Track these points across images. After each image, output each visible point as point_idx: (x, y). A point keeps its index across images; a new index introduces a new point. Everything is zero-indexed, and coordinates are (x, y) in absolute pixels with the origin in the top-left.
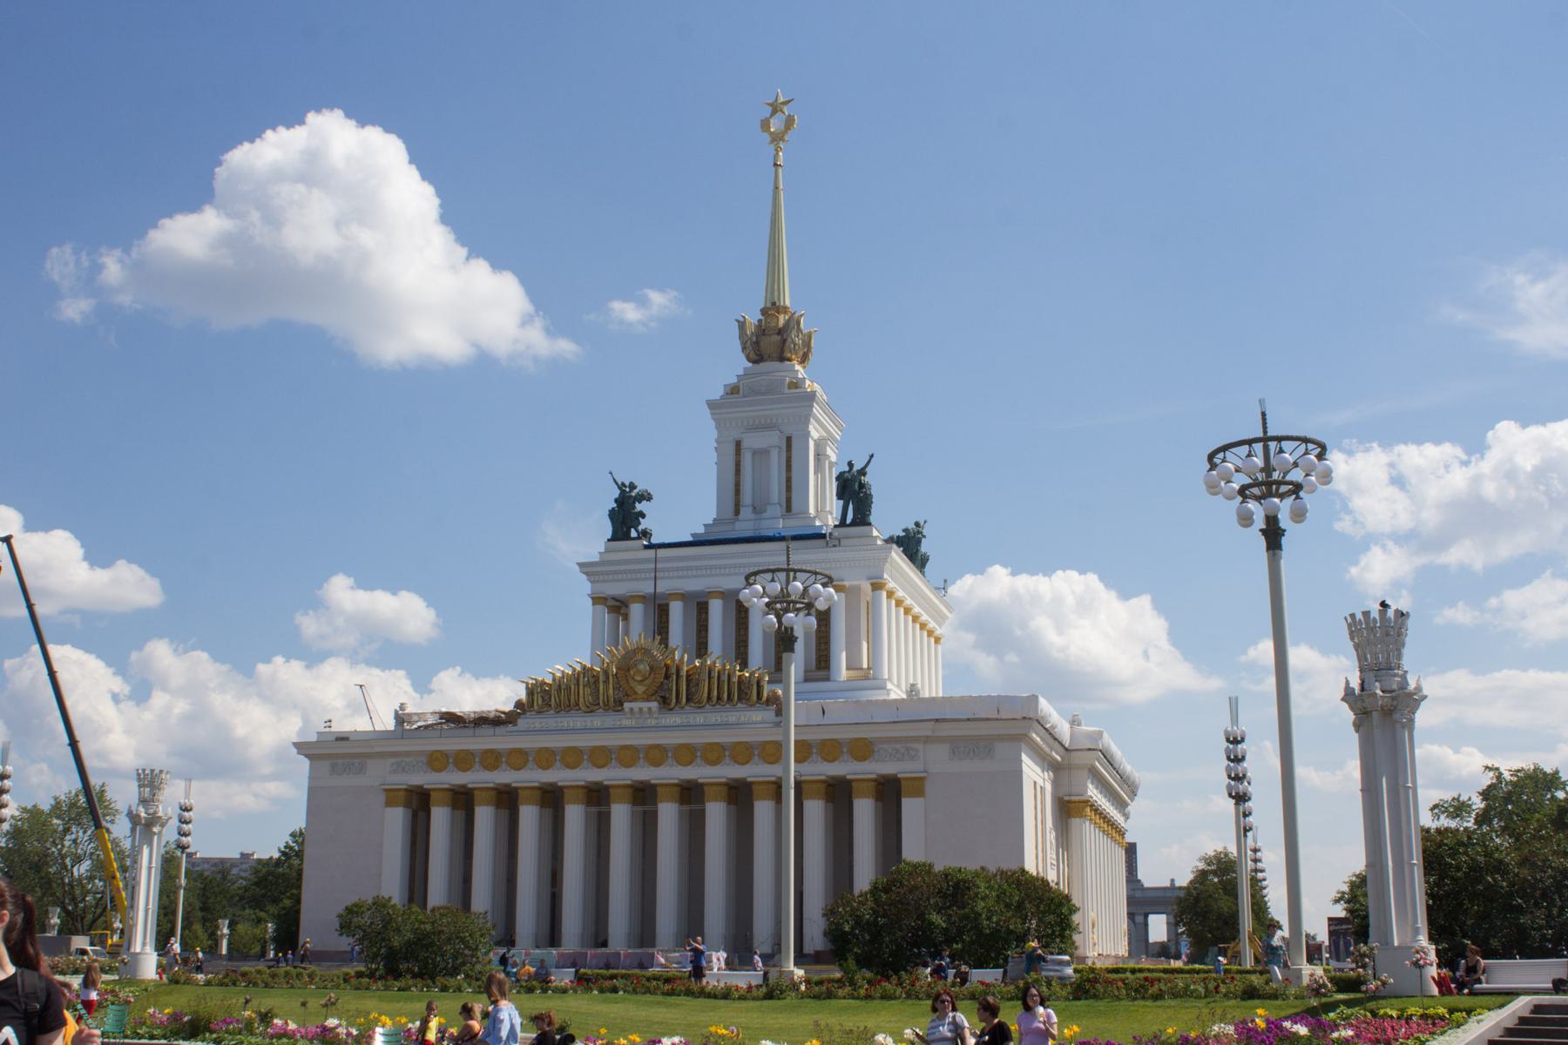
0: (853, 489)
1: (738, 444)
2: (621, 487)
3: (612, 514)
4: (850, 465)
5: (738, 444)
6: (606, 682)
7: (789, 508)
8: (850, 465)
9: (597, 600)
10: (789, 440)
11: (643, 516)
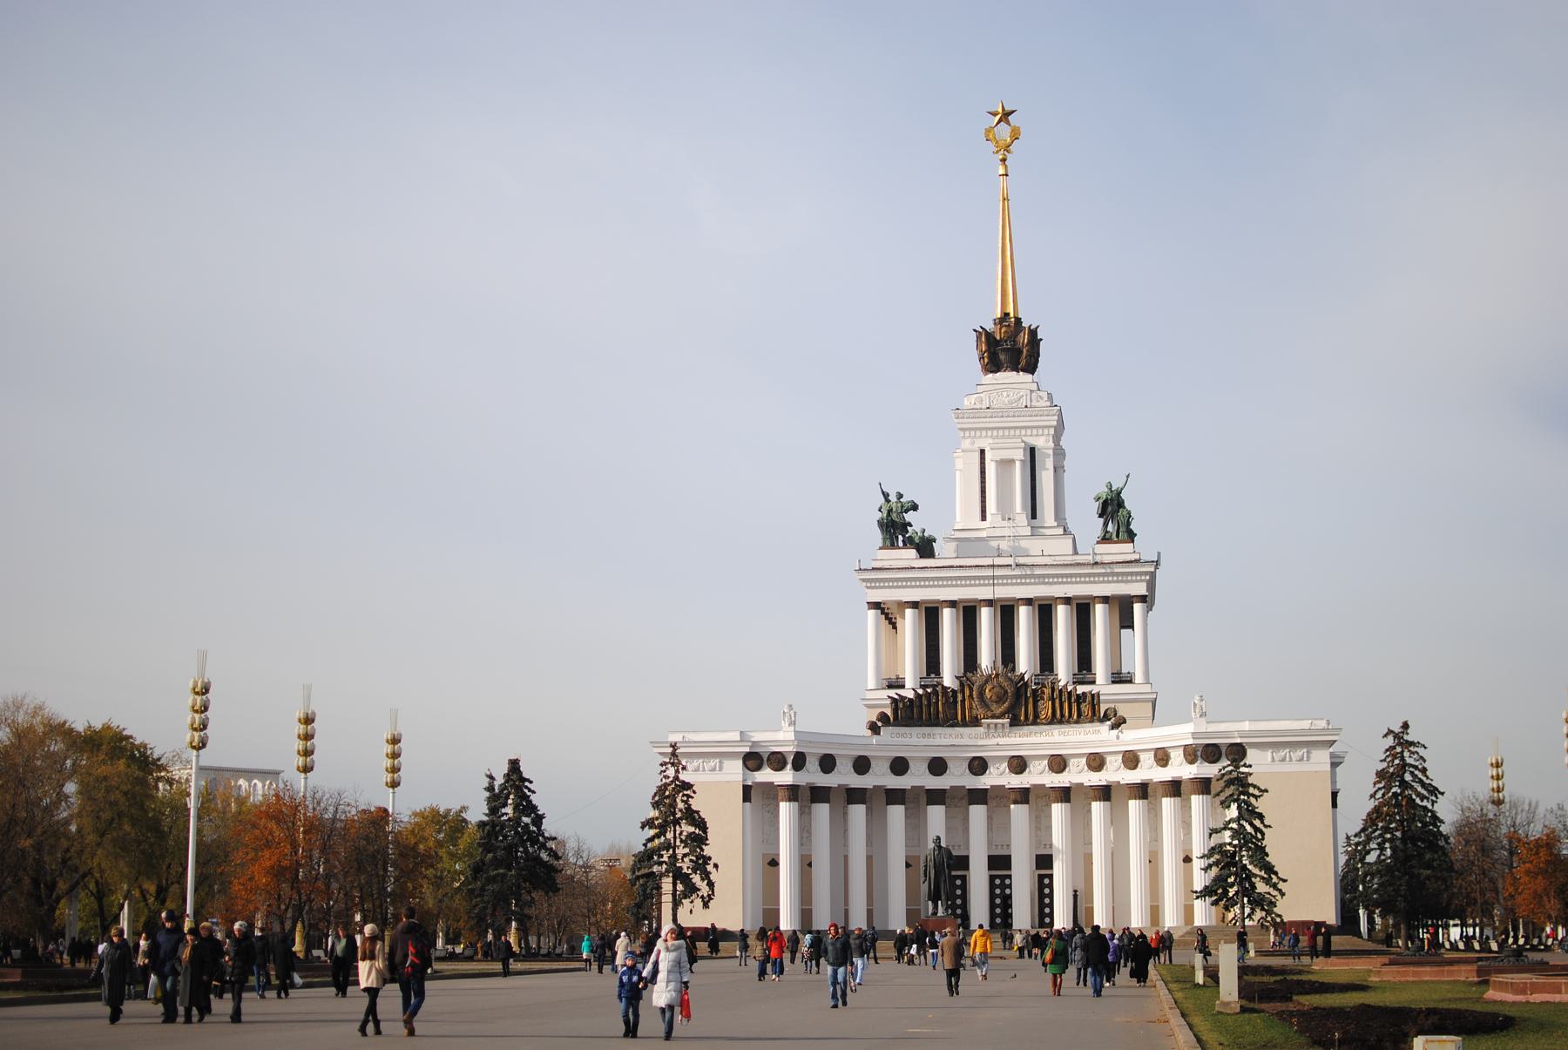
0: (1112, 507)
1: (982, 452)
2: (886, 496)
3: (881, 524)
4: (1110, 486)
6: (963, 701)
7: (1034, 516)
8: (1110, 486)
9: (876, 605)
10: (1032, 450)
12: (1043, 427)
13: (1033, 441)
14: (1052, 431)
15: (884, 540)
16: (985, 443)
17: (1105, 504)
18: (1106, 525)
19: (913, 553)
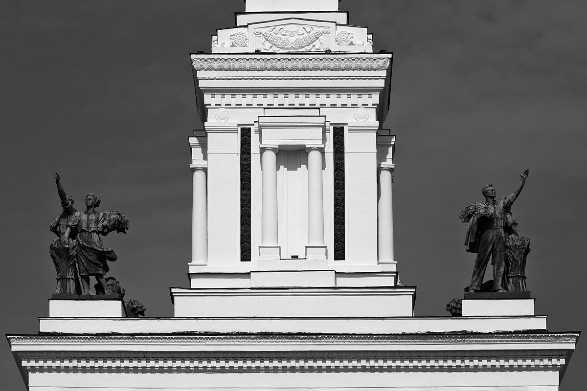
1: (246, 134)
5: (246, 134)
7: (340, 254)
10: (339, 132)
11: (113, 259)
12: (360, 91)
13: (335, 117)
14: (376, 98)
15: (63, 279)
16: (248, 117)
17: (485, 222)
18: (481, 265)
19: (115, 307)
